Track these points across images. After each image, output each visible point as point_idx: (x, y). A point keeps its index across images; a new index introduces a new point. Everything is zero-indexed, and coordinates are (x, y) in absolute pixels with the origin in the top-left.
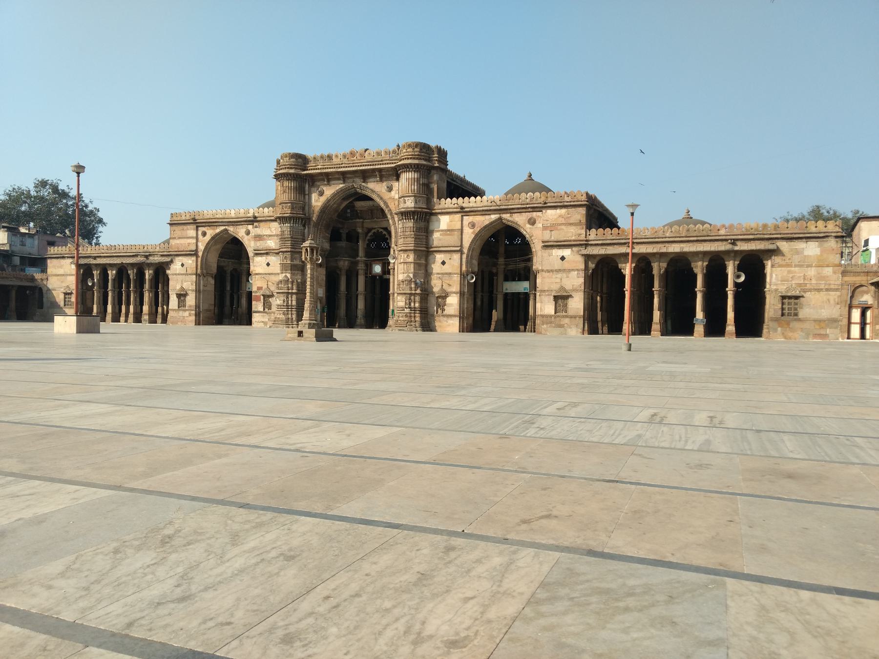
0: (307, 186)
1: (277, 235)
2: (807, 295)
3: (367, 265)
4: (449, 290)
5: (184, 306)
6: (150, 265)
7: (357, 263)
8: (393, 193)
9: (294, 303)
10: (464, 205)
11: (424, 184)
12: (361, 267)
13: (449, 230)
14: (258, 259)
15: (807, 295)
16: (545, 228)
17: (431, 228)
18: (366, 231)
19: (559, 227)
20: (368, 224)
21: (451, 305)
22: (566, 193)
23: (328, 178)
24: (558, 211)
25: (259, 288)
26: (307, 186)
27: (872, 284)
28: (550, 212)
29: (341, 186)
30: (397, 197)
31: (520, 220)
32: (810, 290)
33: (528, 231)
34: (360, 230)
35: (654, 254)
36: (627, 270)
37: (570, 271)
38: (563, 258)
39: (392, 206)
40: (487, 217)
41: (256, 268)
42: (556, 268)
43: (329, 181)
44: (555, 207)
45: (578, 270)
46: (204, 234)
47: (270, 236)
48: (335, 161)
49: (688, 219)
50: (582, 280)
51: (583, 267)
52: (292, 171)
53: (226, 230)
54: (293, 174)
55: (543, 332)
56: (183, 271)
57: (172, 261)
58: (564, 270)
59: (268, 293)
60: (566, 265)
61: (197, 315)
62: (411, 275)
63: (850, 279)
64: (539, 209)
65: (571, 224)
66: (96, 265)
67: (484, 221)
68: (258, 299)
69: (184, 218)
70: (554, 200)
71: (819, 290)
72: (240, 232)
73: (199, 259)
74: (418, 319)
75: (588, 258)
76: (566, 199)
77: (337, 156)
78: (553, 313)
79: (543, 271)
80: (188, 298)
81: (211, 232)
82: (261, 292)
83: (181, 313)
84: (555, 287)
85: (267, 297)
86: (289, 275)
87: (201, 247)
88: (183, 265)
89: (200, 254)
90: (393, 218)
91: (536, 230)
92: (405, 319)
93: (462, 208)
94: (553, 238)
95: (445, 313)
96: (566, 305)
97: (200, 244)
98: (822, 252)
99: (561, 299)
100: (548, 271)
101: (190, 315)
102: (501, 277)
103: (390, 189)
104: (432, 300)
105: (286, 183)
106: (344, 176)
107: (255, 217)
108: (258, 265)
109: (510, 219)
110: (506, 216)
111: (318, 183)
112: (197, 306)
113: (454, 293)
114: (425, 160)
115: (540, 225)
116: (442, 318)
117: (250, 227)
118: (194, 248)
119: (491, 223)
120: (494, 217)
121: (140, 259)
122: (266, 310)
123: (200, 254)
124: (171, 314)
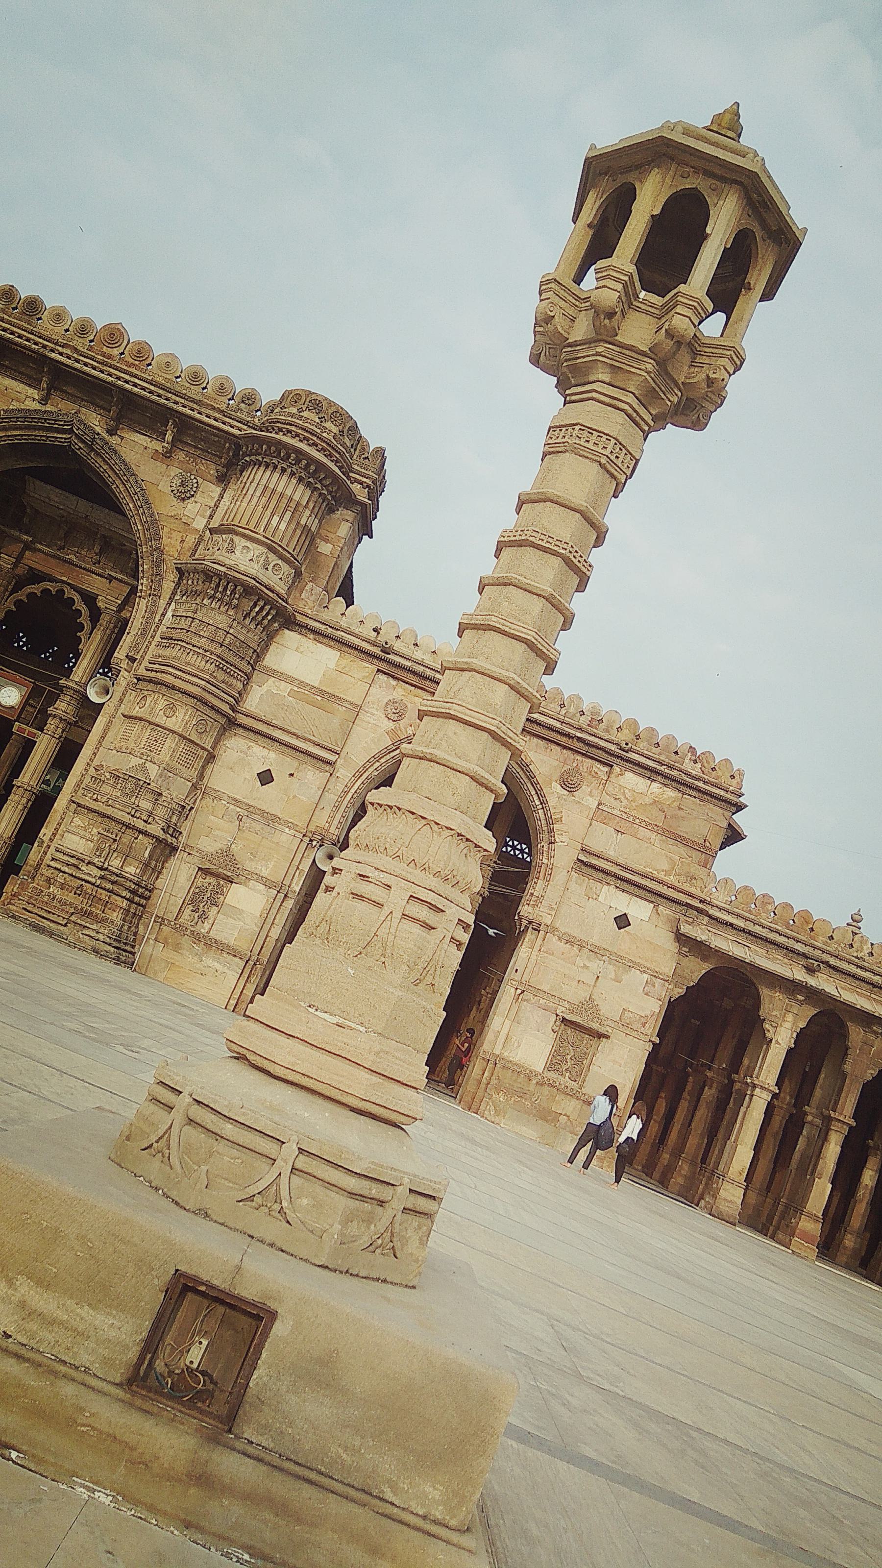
4: (250, 866)
8: (191, 508)
11: (306, 529)
13: (323, 693)
16: (600, 814)
17: (270, 660)
21: (237, 912)
28: (631, 780)
30: (200, 524)
33: (552, 801)
36: (783, 1027)
37: (633, 965)
38: (622, 921)
39: (174, 546)
42: (595, 940)
44: (650, 773)
48: (45, 325)
65: (680, 839)
70: (654, 752)
74: (116, 916)
76: (688, 766)
77: (59, 316)
78: (539, 1066)
84: (575, 994)
90: (158, 577)
92: (70, 897)
94: (611, 854)
95: (204, 928)
96: (579, 1060)
103: (185, 494)
113: (267, 883)
114: (340, 468)
116: (186, 941)
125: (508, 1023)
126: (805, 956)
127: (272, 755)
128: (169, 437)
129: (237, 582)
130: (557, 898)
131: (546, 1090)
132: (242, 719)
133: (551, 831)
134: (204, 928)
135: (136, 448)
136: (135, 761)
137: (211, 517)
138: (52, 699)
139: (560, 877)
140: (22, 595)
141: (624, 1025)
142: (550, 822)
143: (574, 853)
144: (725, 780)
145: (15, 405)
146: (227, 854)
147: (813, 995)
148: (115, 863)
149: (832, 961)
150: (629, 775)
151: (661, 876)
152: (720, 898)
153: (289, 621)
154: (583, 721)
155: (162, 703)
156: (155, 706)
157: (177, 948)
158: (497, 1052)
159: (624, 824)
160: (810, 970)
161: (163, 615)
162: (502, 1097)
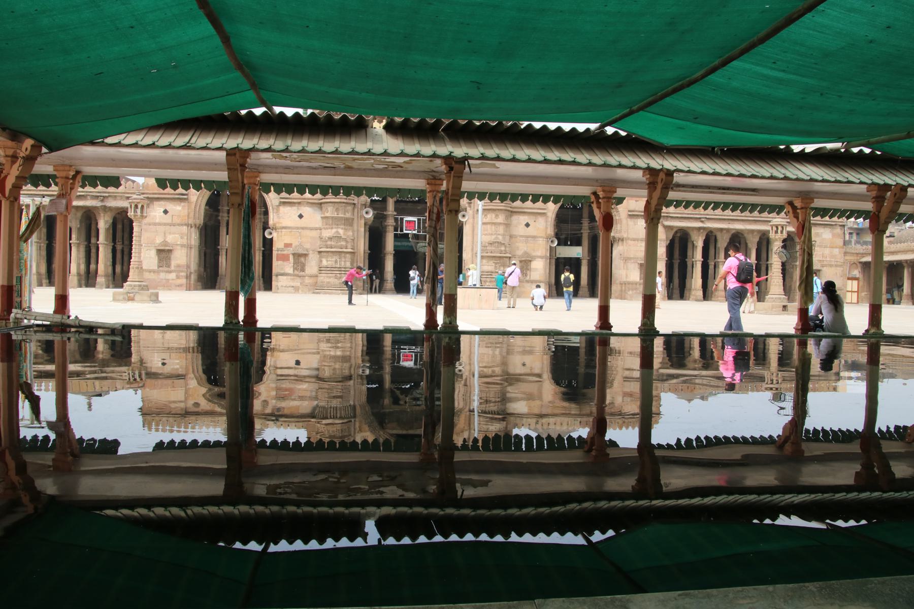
2: (824, 269)
3: (396, 220)
4: (534, 254)
5: (169, 266)
9: (348, 264)
12: (391, 222)
14: (283, 209)
15: (824, 269)
21: (536, 270)
25: (287, 245)
27: (860, 263)
32: (826, 266)
35: (721, 230)
56: (167, 219)
59: (301, 251)
61: (188, 277)
62: (500, 237)
63: (848, 258)
68: (284, 258)
71: (831, 266)
79: (628, 239)
82: (289, 251)
83: (163, 275)
85: (300, 258)
86: (341, 231)
88: (166, 212)
95: (528, 278)
98: (834, 235)
100: (634, 240)
101: (178, 277)
112: (188, 267)
113: (541, 257)
122: (296, 272)
134: (528, 278)
136: (494, 237)
139: (624, 221)
146: (526, 253)
147: (704, 228)
162: (630, 292)
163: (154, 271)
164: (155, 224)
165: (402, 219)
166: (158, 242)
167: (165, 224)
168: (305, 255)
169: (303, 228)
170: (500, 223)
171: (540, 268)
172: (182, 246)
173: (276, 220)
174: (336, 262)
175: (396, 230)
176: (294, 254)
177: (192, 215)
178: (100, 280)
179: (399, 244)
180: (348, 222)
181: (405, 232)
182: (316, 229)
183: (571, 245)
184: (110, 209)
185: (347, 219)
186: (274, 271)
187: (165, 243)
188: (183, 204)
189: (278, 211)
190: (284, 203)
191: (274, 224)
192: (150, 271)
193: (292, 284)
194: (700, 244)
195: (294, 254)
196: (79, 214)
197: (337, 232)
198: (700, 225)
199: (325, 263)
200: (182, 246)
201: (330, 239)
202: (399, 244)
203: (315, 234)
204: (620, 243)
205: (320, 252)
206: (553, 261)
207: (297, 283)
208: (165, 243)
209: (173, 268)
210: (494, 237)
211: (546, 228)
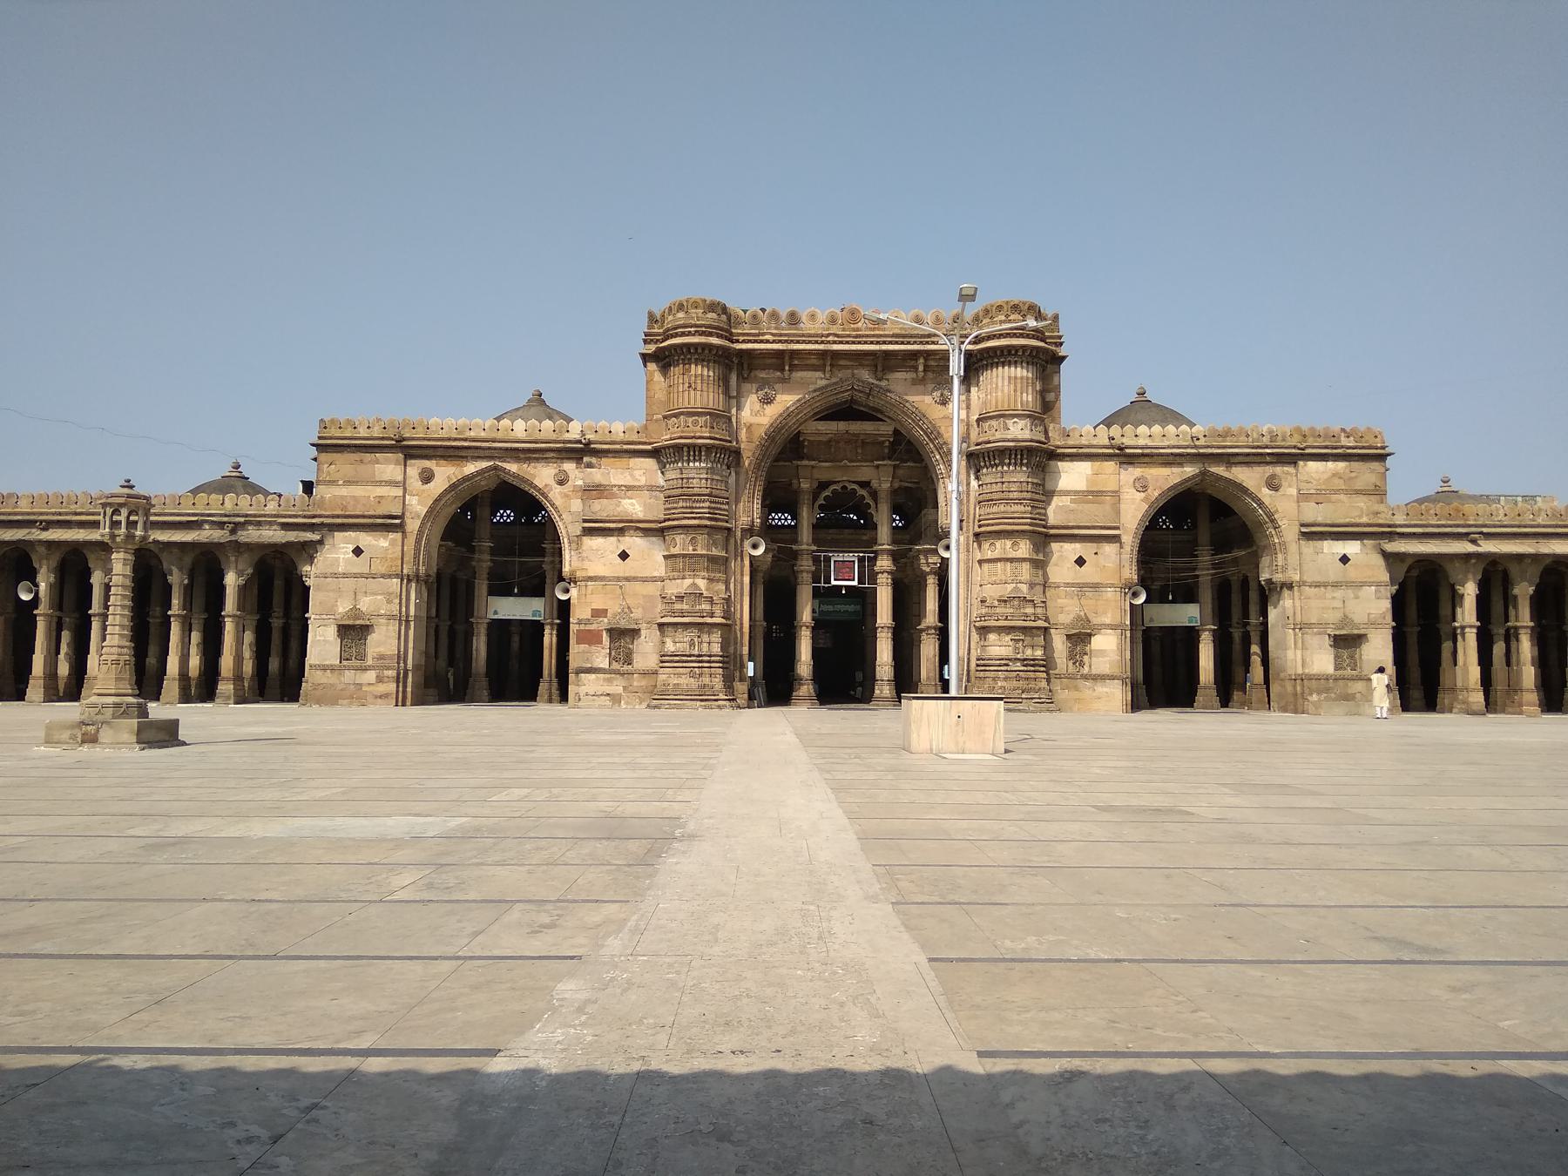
0: (734, 377)
1: (651, 488)
3: (816, 560)
4: (1095, 620)
6: (238, 547)
7: (795, 555)
9: (716, 649)
10: (1127, 441)
12: (806, 565)
18: (816, 485)
19: (1334, 497)
20: (824, 471)
21: (1102, 653)
22: (1343, 430)
23: (784, 363)
24: (1330, 464)
25: (598, 613)
26: (734, 377)
28: (1313, 466)
29: (824, 382)
31: (1248, 477)
33: (1267, 501)
34: (805, 485)
35: (1520, 558)
37: (1363, 584)
38: (1345, 559)
40: (1176, 470)
41: (586, 564)
42: (1332, 578)
43: (793, 368)
45: (1378, 585)
46: (427, 477)
47: (629, 488)
48: (807, 327)
49: (1447, 495)
50: (1385, 605)
51: (1385, 577)
52: (714, 340)
53: (496, 468)
54: (718, 347)
55: (1311, 708)
56: (360, 565)
57: (321, 542)
58: (1349, 584)
59: (623, 624)
60: (1351, 571)
61: (400, 679)
62: (1024, 588)
64: (1291, 459)
65: (1358, 492)
66: (50, 544)
67: (1166, 478)
68: (591, 638)
69: (363, 432)
72: (542, 476)
73: (411, 540)
74: (1044, 684)
75: (1390, 558)
76: (1344, 441)
79: (1302, 584)
80: (372, 638)
81: (446, 474)
82: (604, 623)
83: (349, 676)
84: (1333, 617)
85: (622, 636)
87: (418, 505)
88: (358, 551)
89: (413, 525)
91: (1284, 500)
93: (1120, 449)
94: (1320, 520)
95: (1086, 670)
96: (1352, 657)
97: (412, 501)
99: (1347, 642)
101: (380, 680)
102: (482, 587)
104: (1059, 644)
105: (697, 370)
106: (828, 360)
107: (590, 442)
108: (589, 559)
109: (1226, 474)
110: (1219, 470)
111: (763, 375)
112: (401, 657)
113: (1113, 627)
115: (1294, 491)
116: (1081, 683)
117: (569, 466)
118: (397, 511)
119: (1181, 483)
120: (1190, 470)
121: (218, 535)
122: (616, 666)
123: (413, 525)
124: (312, 677)
125: (1299, 653)
126: (1467, 534)
127: (1078, 545)
128: (921, 368)
129: (1022, 449)
130: (1291, 559)
131: (1341, 683)
132: (1052, 532)
133: (1273, 521)
134: (1086, 670)
135: (898, 381)
136: (1010, 587)
137: (968, 407)
138: (873, 560)
139: (1293, 548)
140: (821, 501)
141: (1373, 624)
142: (1270, 515)
143: (1296, 529)
144: (1372, 442)
145: (812, 387)
146: (1079, 618)
148: (1029, 653)
149: (1485, 530)
150: (1311, 464)
151: (1358, 521)
152: (1400, 519)
153: (1054, 455)
154: (1266, 440)
155: (1009, 543)
156: (1003, 547)
157: (1076, 689)
158: (1300, 671)
159: (1319, 497)
160: (1474, 542)
161: (968, 484)
162: (1315, 697)
163: (332, 669)
164: (335, 575)
165: (828, 560)
166: (341, 610)
167: (356, 576)
168: (634, 633)
169: (627, 579)
170: (1024, 560)
171: (1109, 649)
172: (390, 617)
173: (576, 564)
174: (692, 644)
175: (816, 579)
176: (610, 631)
177: (409, 557)
178: (225, 687)
179: (825, 608)
180: (718, 565)
181: (834, 583)
182: (654, 580)
183: (1173, 602)
184: (249, 547)
185: (713, 560)
186: (574, 663)
187: (355, 612)
188: (392, 536)
189: (579, 545)
190: (589, 532)
191: (573, 572)
192: (324, 668)
193: (609, 689)
194: (1470, 591)
195: (610, 631)
196: (188, 560)
197: (694, 584)
198: (1469, 548)
199: (670, 646)
200: (390, 617)
201: (680, 598)
202: (825, 608)
203: (652, 589)
204: (1286, 593)
205: (661, 625)
206: (1139, 634)
207: (617, 687)
208: (355, 612)
209: (370, 662)
210: (1010, 587)
211: (1121, 566)
